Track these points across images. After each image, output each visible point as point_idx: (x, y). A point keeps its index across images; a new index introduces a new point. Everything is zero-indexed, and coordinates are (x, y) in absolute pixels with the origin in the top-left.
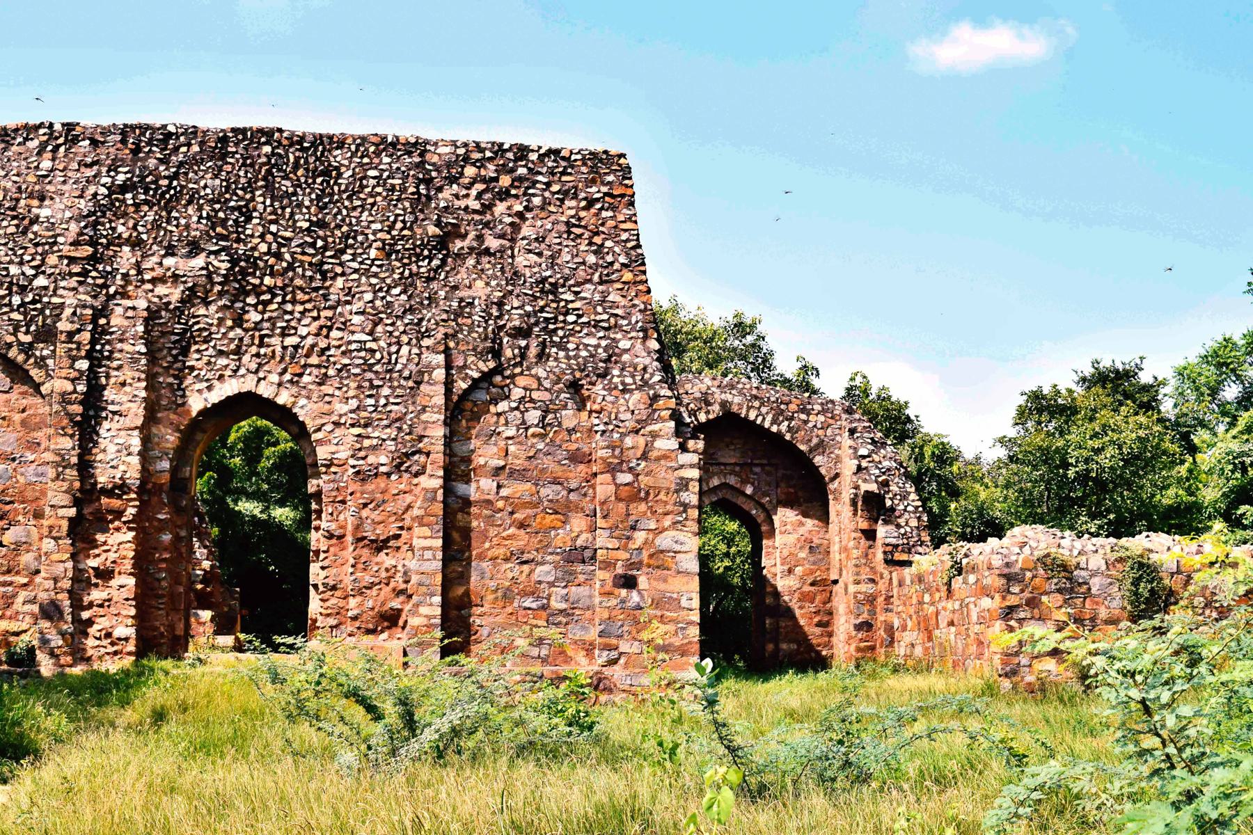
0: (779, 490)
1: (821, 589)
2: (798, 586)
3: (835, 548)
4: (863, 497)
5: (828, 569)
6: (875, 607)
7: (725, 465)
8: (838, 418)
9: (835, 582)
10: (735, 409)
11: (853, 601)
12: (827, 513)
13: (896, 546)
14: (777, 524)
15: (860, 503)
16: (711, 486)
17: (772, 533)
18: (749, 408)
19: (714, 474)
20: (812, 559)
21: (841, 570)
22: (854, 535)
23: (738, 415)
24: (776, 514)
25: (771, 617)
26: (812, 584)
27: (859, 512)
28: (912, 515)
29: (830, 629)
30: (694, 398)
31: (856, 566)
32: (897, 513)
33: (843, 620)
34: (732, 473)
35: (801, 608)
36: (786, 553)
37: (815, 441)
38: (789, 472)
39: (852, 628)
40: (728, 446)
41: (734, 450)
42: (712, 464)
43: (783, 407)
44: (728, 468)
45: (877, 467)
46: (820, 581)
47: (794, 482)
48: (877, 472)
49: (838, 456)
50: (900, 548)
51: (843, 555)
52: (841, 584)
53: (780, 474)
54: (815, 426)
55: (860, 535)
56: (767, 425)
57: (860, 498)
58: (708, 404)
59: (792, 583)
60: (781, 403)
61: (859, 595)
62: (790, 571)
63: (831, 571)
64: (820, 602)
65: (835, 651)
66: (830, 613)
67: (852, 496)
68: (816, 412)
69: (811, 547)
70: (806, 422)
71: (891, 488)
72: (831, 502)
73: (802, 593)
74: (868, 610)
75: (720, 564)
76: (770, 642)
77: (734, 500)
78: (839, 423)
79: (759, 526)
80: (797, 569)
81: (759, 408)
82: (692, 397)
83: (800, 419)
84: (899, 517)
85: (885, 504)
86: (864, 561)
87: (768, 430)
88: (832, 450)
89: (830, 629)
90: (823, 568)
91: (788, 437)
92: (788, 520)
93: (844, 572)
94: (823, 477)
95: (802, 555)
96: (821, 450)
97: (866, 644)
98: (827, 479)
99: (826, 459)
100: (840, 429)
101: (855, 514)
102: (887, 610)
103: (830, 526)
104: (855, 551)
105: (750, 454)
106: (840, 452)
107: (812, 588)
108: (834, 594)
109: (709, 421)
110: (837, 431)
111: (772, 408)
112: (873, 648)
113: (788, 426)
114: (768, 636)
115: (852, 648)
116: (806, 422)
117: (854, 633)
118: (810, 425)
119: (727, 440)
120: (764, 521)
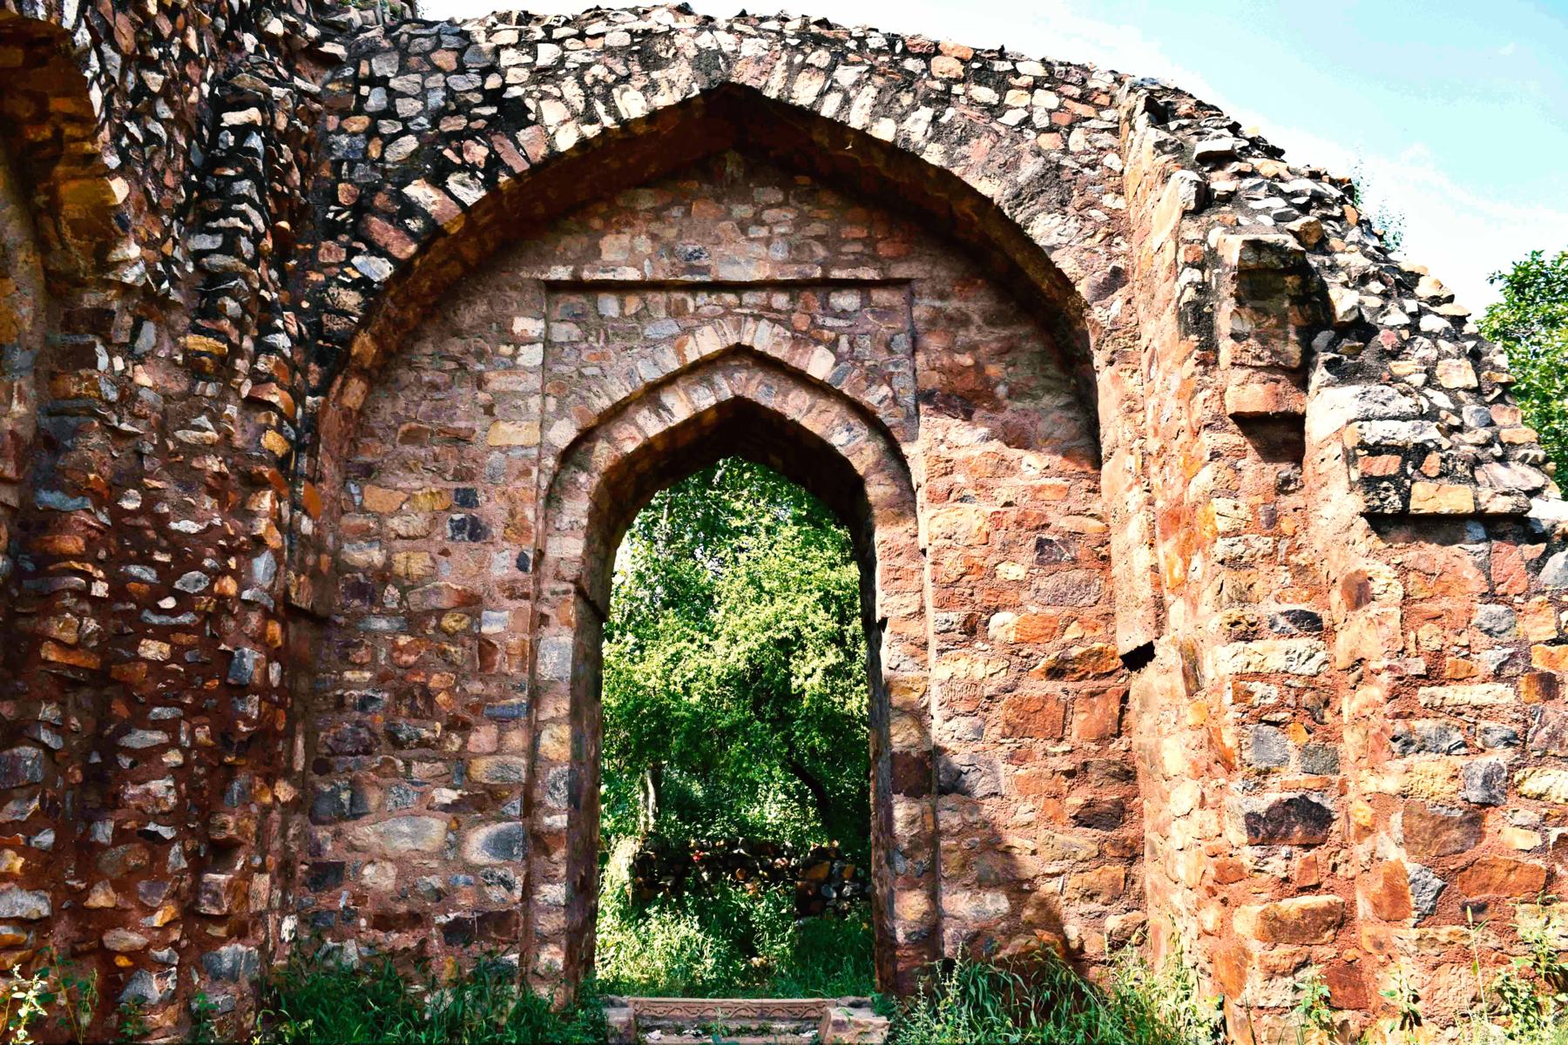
0: (921, 358)
1: (1089, 685)
2: (1001, 680)
3: (1128, 542)
4: (1244, 274)
5: (1108, 617)
6: (1332, 737)
7: (738, 288)
8: (1104, 100)
9: (1140, 658)
10: (745, 75)
11: (1232, 714)
12: (1091, 428)
13: (1422, 450)
14: (919, 472)
15: (1225, 320)
16: (692, 357)
17: (905, 504)
18: (793, 71)
19: (702, 319)
20: (1047, 584)
21: (1160, 605)
22: (1208, 440)
23: (754, 94)
24: (913, 438)
25: (913, 793)
26: (1055, 672)
27: (1227, 348)
28: (1445, 345)
29: (1128, 832)
30: (609, 51)
31: (1234, 563)
32: (1385, 340)
33: (1184, 795)
34: (764, 312)
35: (1015, 758)
36: (952, 565)
37: (1030, 168)
38: (951, 306)
39: (1236, 833)
40: (743, 227)
41: (768, 242)
42: (693, 288)
43: (911, 64)
44: (749, 298)
45: (1274, 191)
46: (1082, 658)
47: (973, 334)
48: (1278, 204)
49: (1113, 216)
50: (1433, 462)
51: (1166, 548)
52: (1166, 654)
53: (922, 310)
54: (1027, 122)
55: (1232, 437)
56: (857, 118)
57: (1227, 289)
58: (651, 62)
59: (979, 671)
60: (906, 52)
61: (1258, 687)
62: (972, 629)
63: (1120, 619)
64: (1083, 732)
65: (1155, 918)
66: (1127, 775)
67: (1190, 294)
68: (1026, 81)
69: (1041, 544)
70: (995, 111)
71: (1341, 259)
72: (1104, 378)
73: (1018, 706)
74: (1305, 752)
75: (816, 662)
76: (912, 886)
77: (772, 402)
78: (1107, 114)
79: (859, 483)
80: (997, 619)
81: (831, 69)
82: (598, 44)
83: (972, 103)
84: (1394, 355)
85: (1328, 305)
86: (1262, 544)
87: (863, 136)
88: (1092, 193)
89: (1128, 832)
90: (1089, 614)
91: (934, 155)
92: (958, 455)
93: (1177, 610)
94: (1065, 284)
95: (1012, 571)
96: (1053, 195)
97: (1308, 901)
98: (1083, 289)
99: (1073, 224)
100: (1115, 132)
101: (1208, 357)
102: (1406, 743)
103: (1105, 467)
104: (1223, 504)
105: (820, 252)
106: (1120, 203)
107: (1055, 687)
108: (1134, 704)
109: (654, 116)
110: (1106, 140)
111: (872, 70)
112: (1340, 919)
113: (935, 119)
114: (901, 865)
115: (1246, 921)
116: (995, 111)
117: (1248, 856)
118: (1012, 118)
119: (743, 211)
120: (878, 467)
